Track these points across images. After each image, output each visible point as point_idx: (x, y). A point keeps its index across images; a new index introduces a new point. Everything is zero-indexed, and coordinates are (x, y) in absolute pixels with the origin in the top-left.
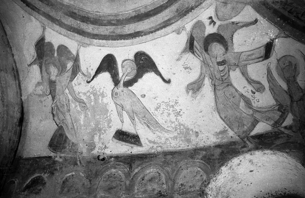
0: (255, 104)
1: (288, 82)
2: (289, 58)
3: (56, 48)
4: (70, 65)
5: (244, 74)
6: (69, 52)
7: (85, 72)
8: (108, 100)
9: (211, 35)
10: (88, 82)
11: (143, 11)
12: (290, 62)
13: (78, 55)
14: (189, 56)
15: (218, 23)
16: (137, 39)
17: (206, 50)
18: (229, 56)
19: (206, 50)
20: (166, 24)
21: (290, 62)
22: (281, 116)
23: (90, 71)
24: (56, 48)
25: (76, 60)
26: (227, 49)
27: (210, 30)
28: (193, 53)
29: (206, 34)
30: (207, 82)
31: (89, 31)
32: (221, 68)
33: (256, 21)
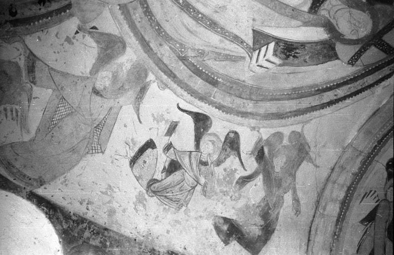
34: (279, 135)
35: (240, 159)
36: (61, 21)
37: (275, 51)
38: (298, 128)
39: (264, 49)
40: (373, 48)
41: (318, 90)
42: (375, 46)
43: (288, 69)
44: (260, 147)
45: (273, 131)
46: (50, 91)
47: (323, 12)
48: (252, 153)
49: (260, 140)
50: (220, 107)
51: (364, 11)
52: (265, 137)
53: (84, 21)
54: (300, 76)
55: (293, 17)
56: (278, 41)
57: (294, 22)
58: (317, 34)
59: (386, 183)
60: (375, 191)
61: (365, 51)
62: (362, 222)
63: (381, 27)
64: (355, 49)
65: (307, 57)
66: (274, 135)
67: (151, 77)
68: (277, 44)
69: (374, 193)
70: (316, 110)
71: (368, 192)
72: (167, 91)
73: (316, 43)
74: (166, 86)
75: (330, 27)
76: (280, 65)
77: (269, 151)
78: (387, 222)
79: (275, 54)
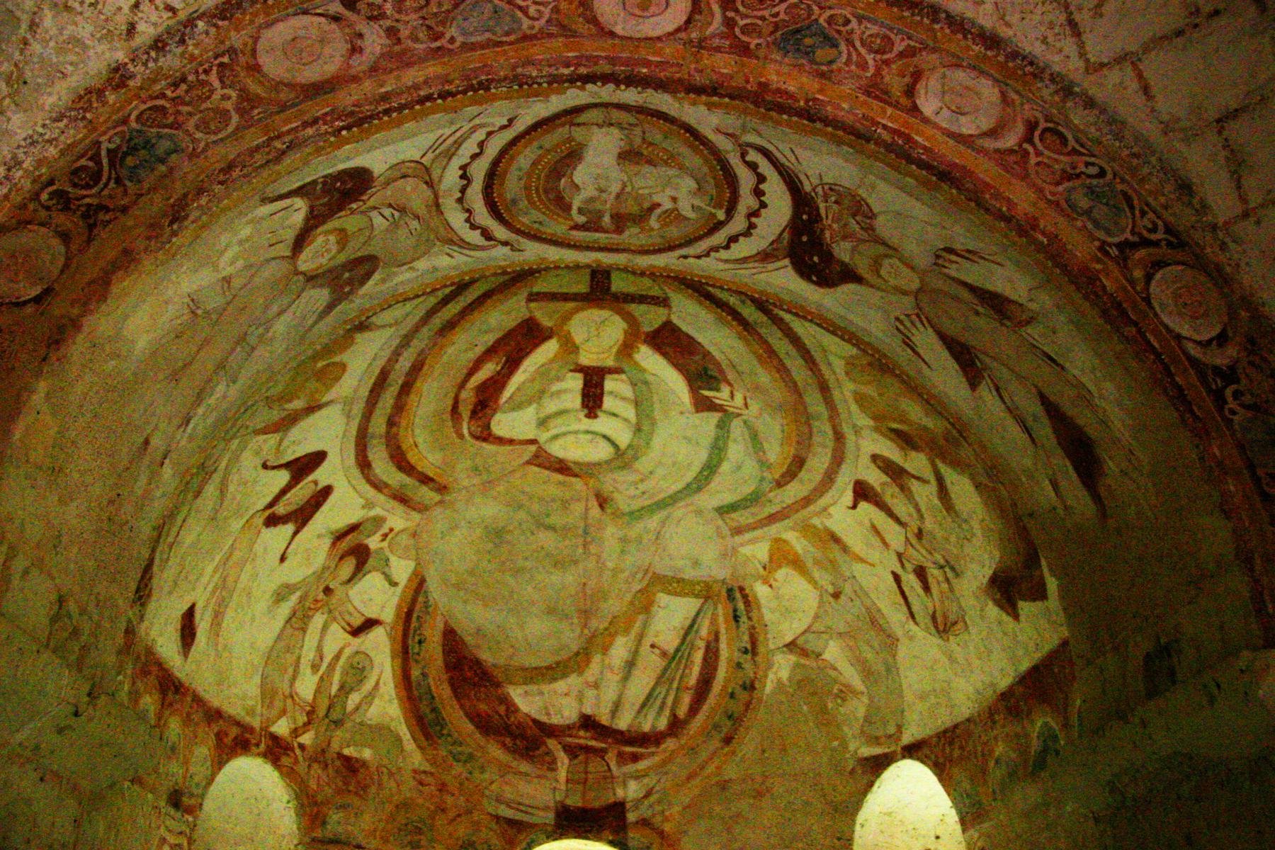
0: (297, 684)
1: (342, 687)
2: (367, 663)
3: (336, 359)
4: (298, 404)
5: (325, 628)
6: (328, 388)
7: (285, 443)
8: (236, 525)
9: (366, 548)
10: (265, 466)
11: (412, 457)
12: (364, 667)
13: (320, 407)
14: (327, 542)
15: (385, 544)
16: (356, 472)
17: (341, 559)
18: (339, 592)
19: (341, 559)
20: (378, 485)
21: (364, 667)
22: (305, 725)
23: (290, 451)
24: (336, 359)
25: (311, 409)
26: (350, 580)
27: (373, 543)
28: (334, 544)
29: (366, 542)
30: (294, 599)
31: (380, 405)
32: (321, 596)
33: (394, 584)
34: (860, 399)
35: (914, 477)
36: (756, 599)
37: (710, 389)
38: (839, 365)
39: (717, 401)
40: (614, 289)
41: (745, 329)
42: (609, 288)
43: (731, 376)
44: (893, 436)
45: (854, 407)
46: (831, 643)
47: (610, 363)
48: (902, 448)
49: (877, 429)
50: (838, 459)
51: (569, 333)
52: (871, 423)
53: (759, 577)
54: (733, 357)
55: (646, 383)
56: (694, 390)
57: (649, 378)
58: (648, 358)
59: (872, 286)
60: (897, 319)
61: (628, 295)
62: (973, 386)
63: (570, 305)
64: (638, 310)
65: (697, 358)
66: (861, 406)
67: (816, 521)
68: (700, 388)
69: (902, 322)
70: (790, 328)
71: (900, 336)
72: (832, 510)
73: (664, 354)
74: (825, 509)
75: (627, 349)
76: (730, 384)
77: (894, 420)
78: (977, 313)
79: (718, 390)
